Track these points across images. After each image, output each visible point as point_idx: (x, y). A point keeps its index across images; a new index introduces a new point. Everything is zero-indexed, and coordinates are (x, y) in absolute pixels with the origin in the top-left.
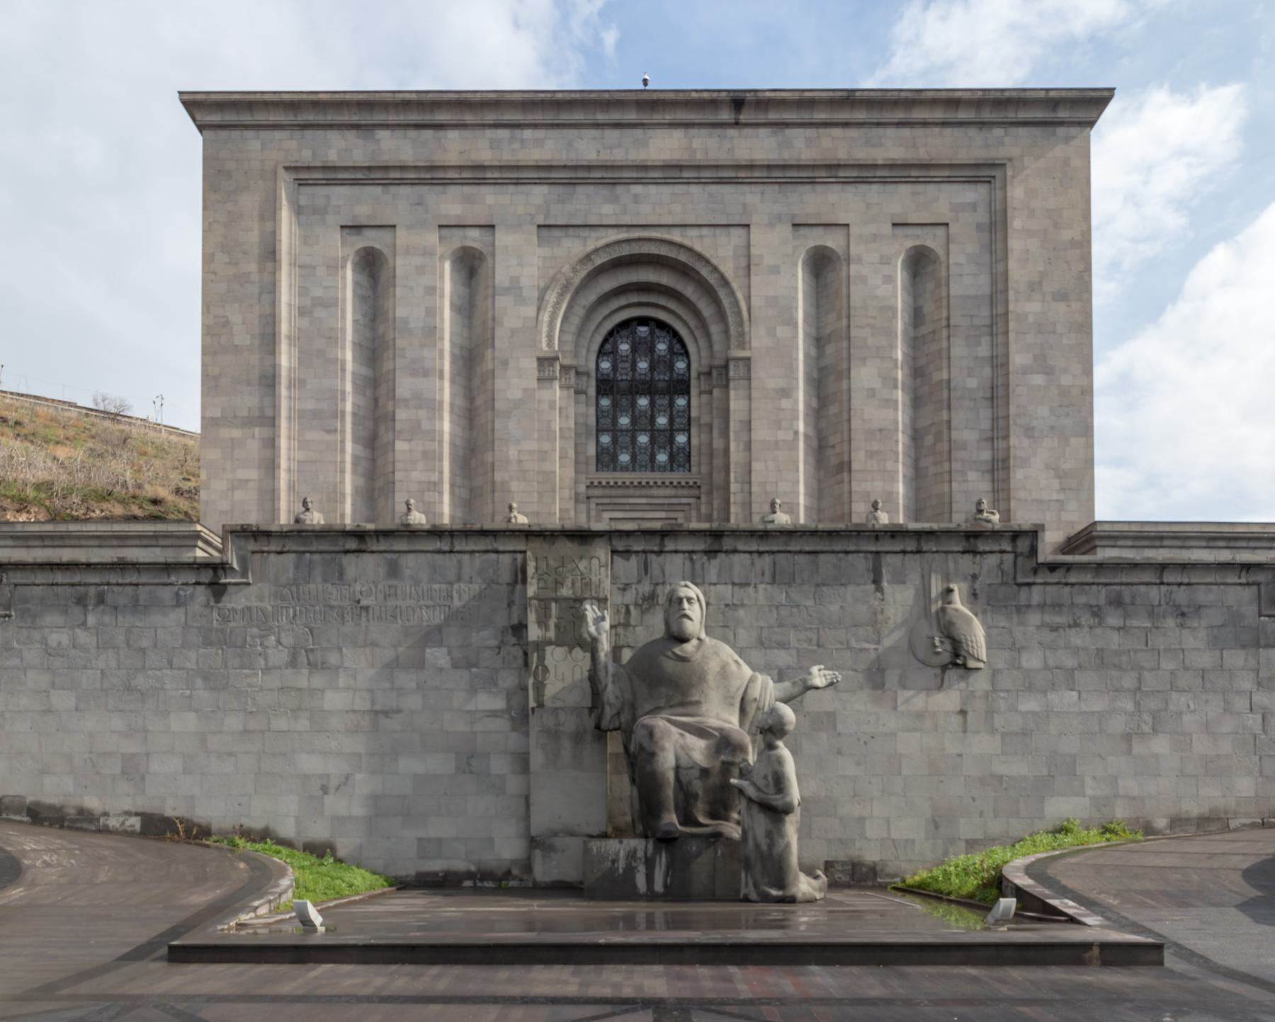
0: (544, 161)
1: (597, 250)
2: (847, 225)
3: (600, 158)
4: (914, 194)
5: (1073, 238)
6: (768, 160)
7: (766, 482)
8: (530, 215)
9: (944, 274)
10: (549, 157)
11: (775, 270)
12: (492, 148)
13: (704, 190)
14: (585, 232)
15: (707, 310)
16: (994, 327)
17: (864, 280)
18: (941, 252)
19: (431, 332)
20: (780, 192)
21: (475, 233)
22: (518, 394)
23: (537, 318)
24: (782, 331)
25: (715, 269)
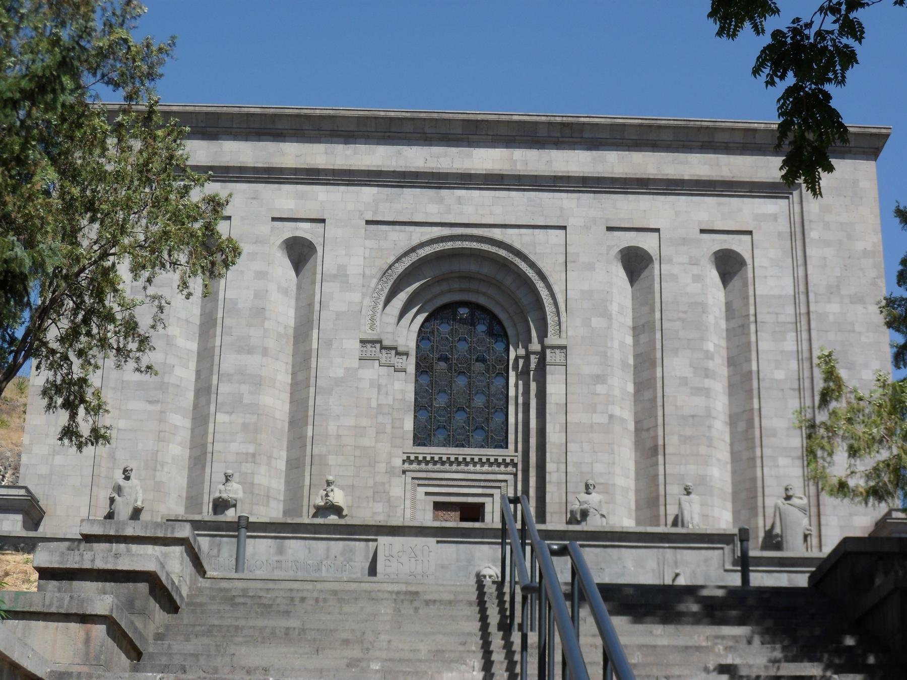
0: (374, 166)
1: (422, 245)
2: (657, 230)
3: (427, 165)
4: (719, 204)
5: (865, 249)
6: (583, 172)
7: (581, 463)
8: (360, 211)
9: (750, 275)
10: (380, 163)
11: (591, 267)
12: (326, 153)
13: (524, 195)
14: (412, 228)
15: (525, 300)
16: (798, 324)
17: (674, 278)
18: (747, 256)
19: (259, 313)
20: (594, 199)
21: (307, 225)
22: (340, 373)
23: (362, 302)
24: (597, 322)
25: (532, 265)
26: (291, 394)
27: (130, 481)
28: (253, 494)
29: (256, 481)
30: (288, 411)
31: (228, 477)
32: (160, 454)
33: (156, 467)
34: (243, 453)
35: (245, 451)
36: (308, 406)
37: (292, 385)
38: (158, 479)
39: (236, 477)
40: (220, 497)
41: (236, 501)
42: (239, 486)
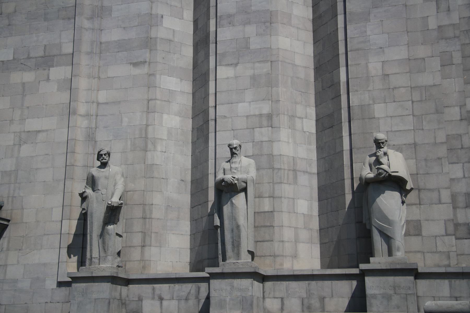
26: (314, 31)
27: (107, 169)
28: (273, 169)
29: (275, 152)
30: (312, 55)
31: (234, 150)
32: (150, 128)
33: (146, 146)
34: (255, 115)
35: (257, 113)
36: (337, 42)
37: (314, 20)
38: (149, 162)
39: (248, 148)
40: (223, 180)
41: (246, 183)
42: (252, 161)
